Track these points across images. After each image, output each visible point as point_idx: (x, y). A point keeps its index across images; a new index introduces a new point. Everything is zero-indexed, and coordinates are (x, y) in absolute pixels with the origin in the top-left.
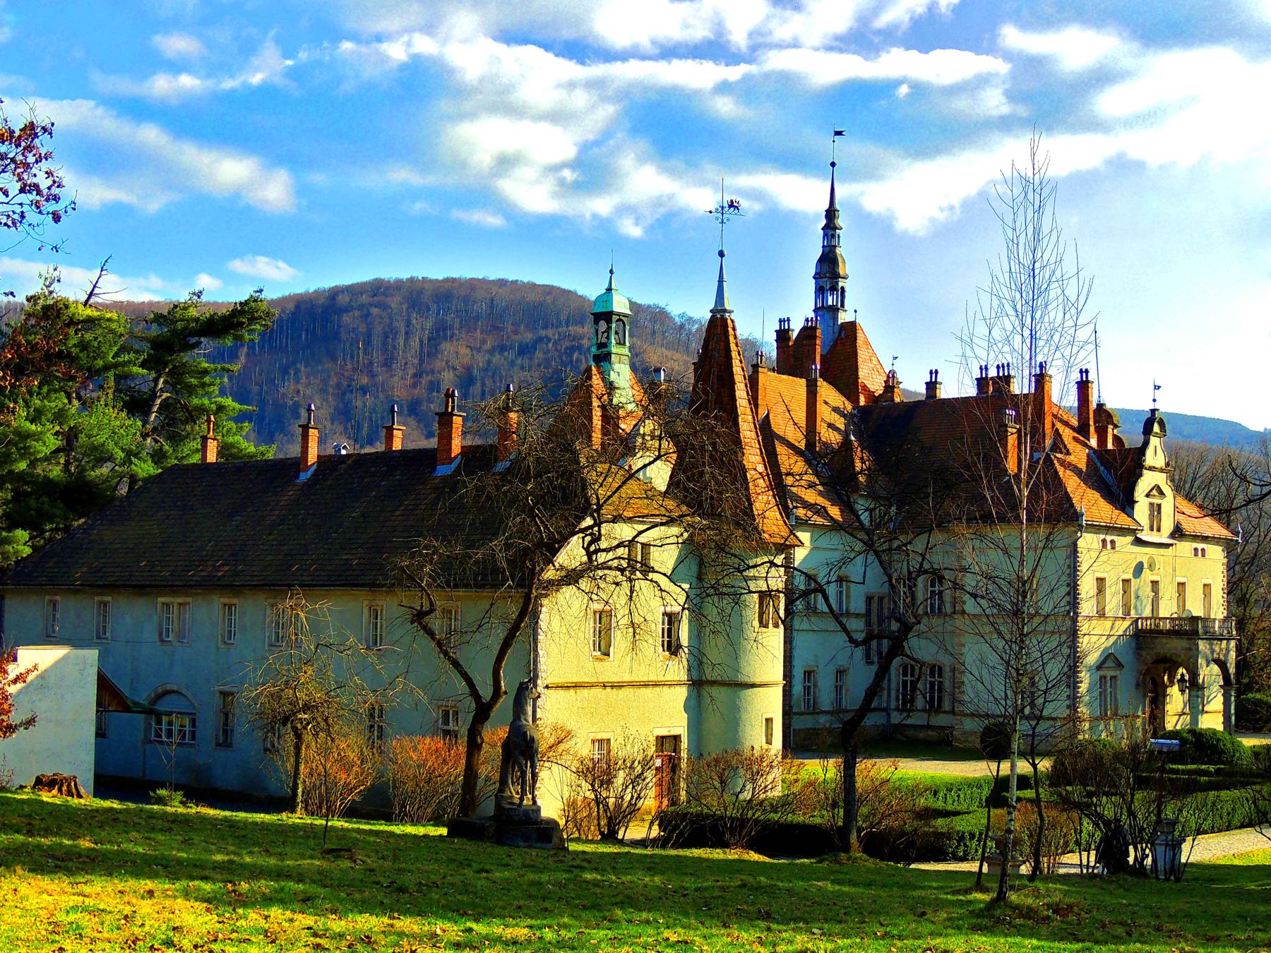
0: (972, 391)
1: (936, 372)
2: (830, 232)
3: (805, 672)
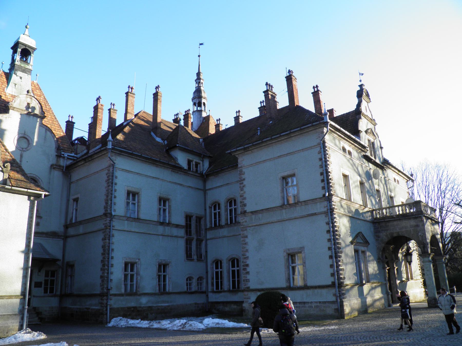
0: (257, 114)
1: (239, 111)
2: (198, 81)
3: (126, 264)
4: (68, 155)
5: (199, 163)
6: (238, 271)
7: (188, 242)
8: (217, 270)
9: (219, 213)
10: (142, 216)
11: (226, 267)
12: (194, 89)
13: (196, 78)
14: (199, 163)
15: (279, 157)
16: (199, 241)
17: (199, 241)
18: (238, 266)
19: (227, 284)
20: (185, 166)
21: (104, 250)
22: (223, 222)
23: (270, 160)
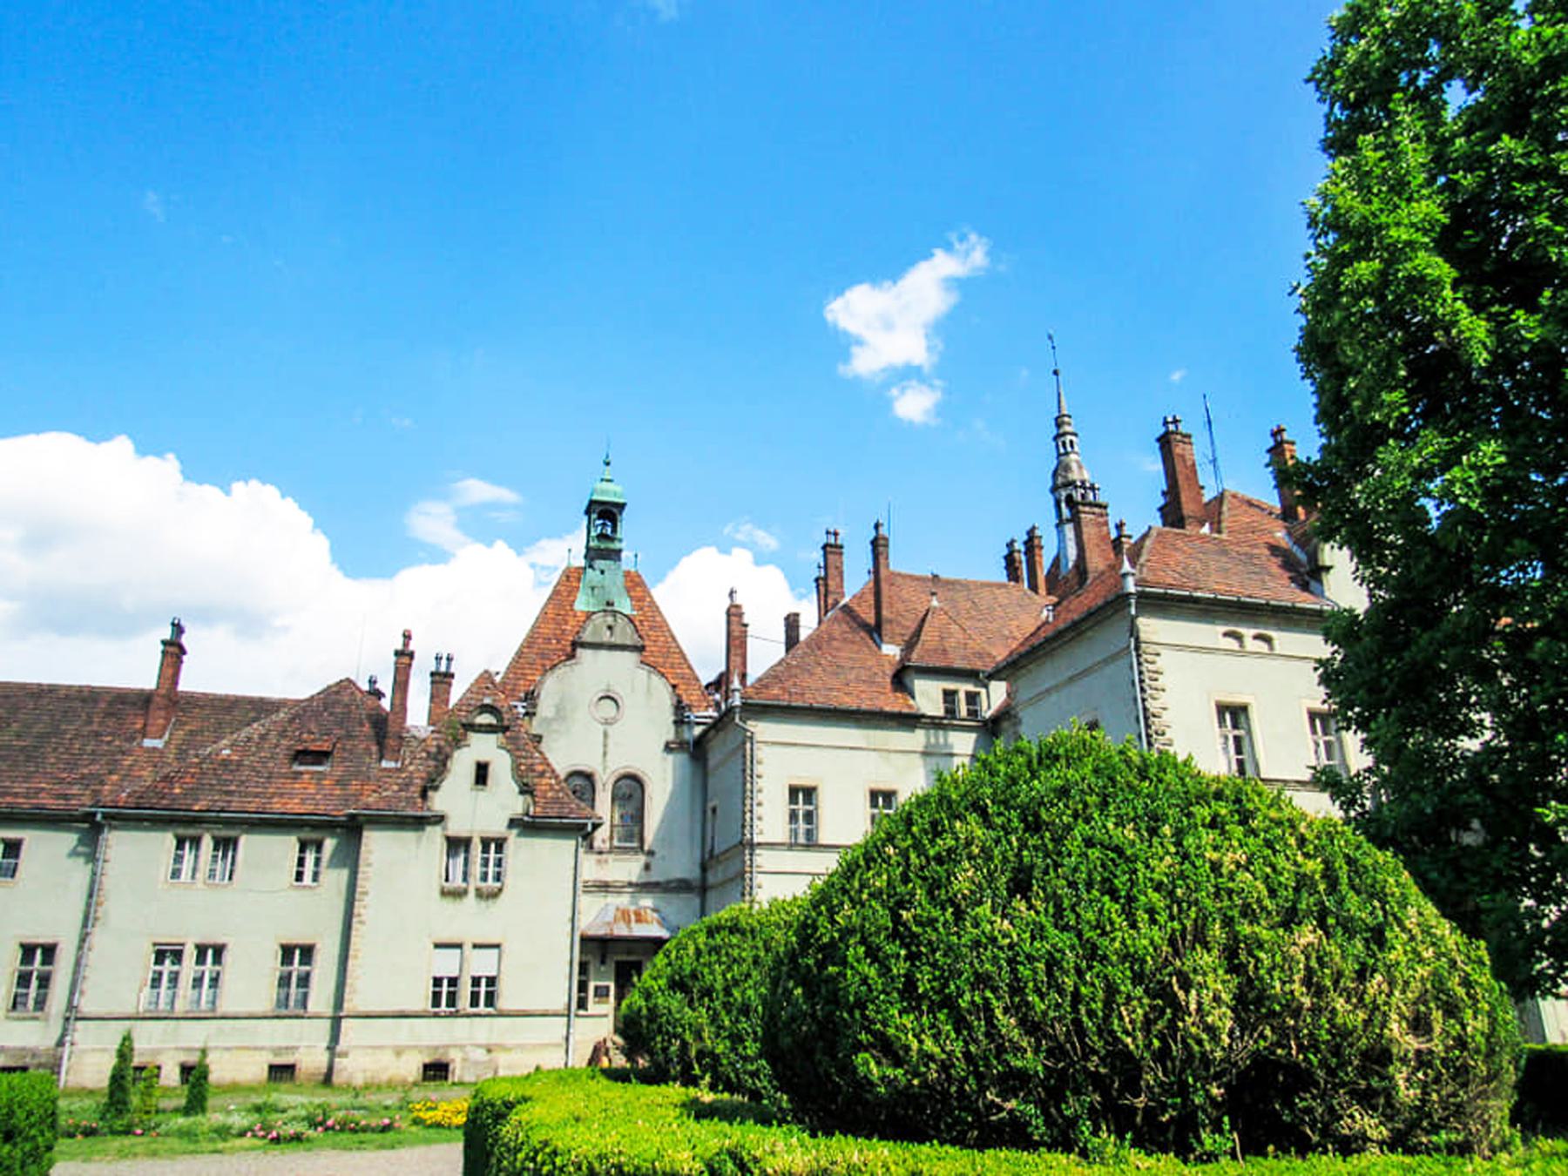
5: (978, 694)
14: (978, 694)
15: (1071, 679)
20: (938, 710)
23: (1056, 688)
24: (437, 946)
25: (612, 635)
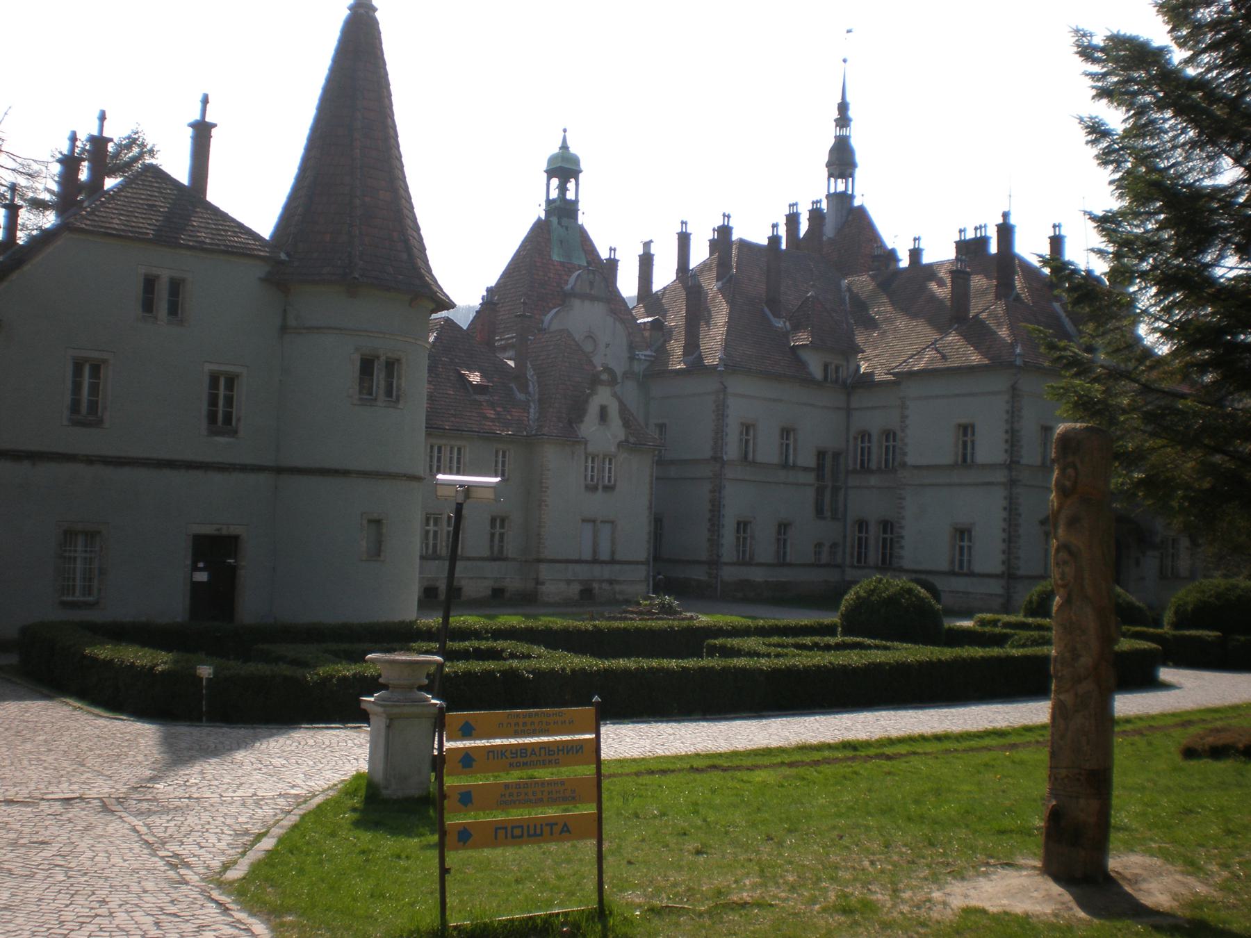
3: (739, 524)
4: (645, 356)
6: (891, 539)
7: (820, 492)
8: (860, 535)
9: (869, 448)
10: (759, 459)
11: (874, 532)
12: (832, 141)
13: (836, 115)
15: (958, 395)
16: (836, 490)
17: (836, 490)
18: (892, 533)
19: (873, 556)
21: (713, 506)
22: (874, 466)
24: (584, 521)
25: (591, 289)
